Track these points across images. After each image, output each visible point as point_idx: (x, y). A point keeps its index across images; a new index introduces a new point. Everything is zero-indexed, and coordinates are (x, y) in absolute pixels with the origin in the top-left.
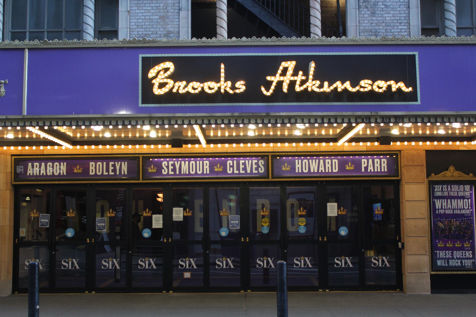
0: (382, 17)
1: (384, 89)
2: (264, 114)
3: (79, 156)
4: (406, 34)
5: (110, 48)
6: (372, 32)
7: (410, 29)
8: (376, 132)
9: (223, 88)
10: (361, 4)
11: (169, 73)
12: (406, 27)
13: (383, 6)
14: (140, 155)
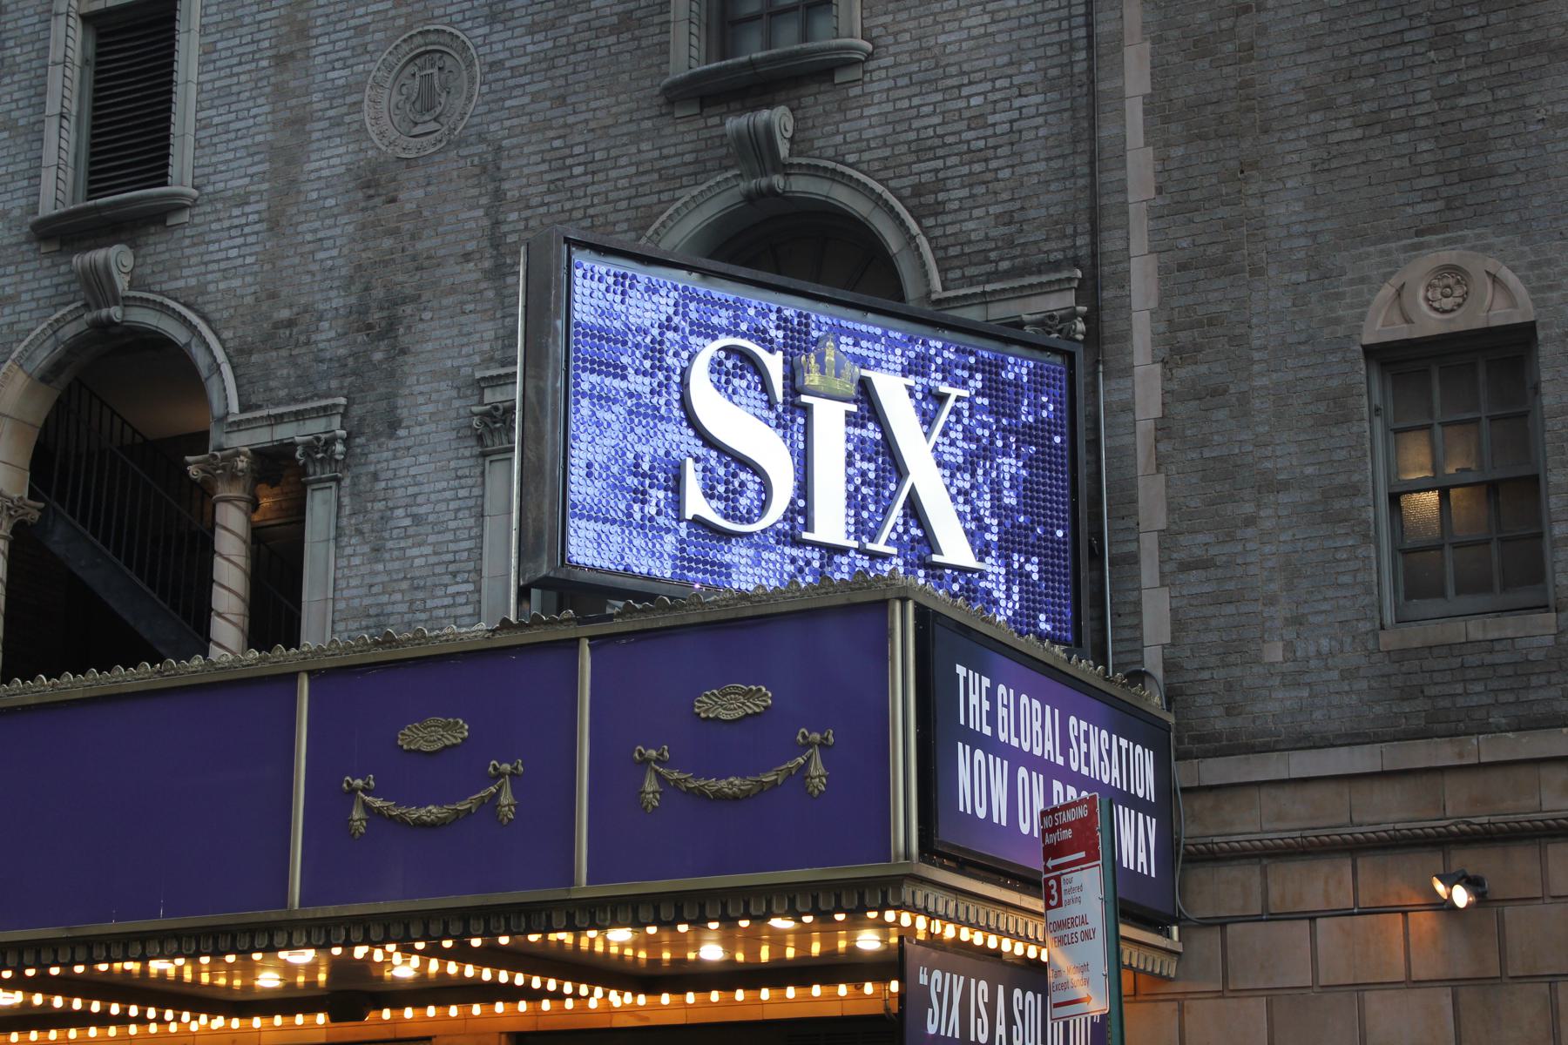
0: (404, 558)
4: (469, 609)
6: (369, 616)
7: (479, 591)
8: (322, 977)
10: (344, 522)
12: (471, 587)
13: (408, 522)
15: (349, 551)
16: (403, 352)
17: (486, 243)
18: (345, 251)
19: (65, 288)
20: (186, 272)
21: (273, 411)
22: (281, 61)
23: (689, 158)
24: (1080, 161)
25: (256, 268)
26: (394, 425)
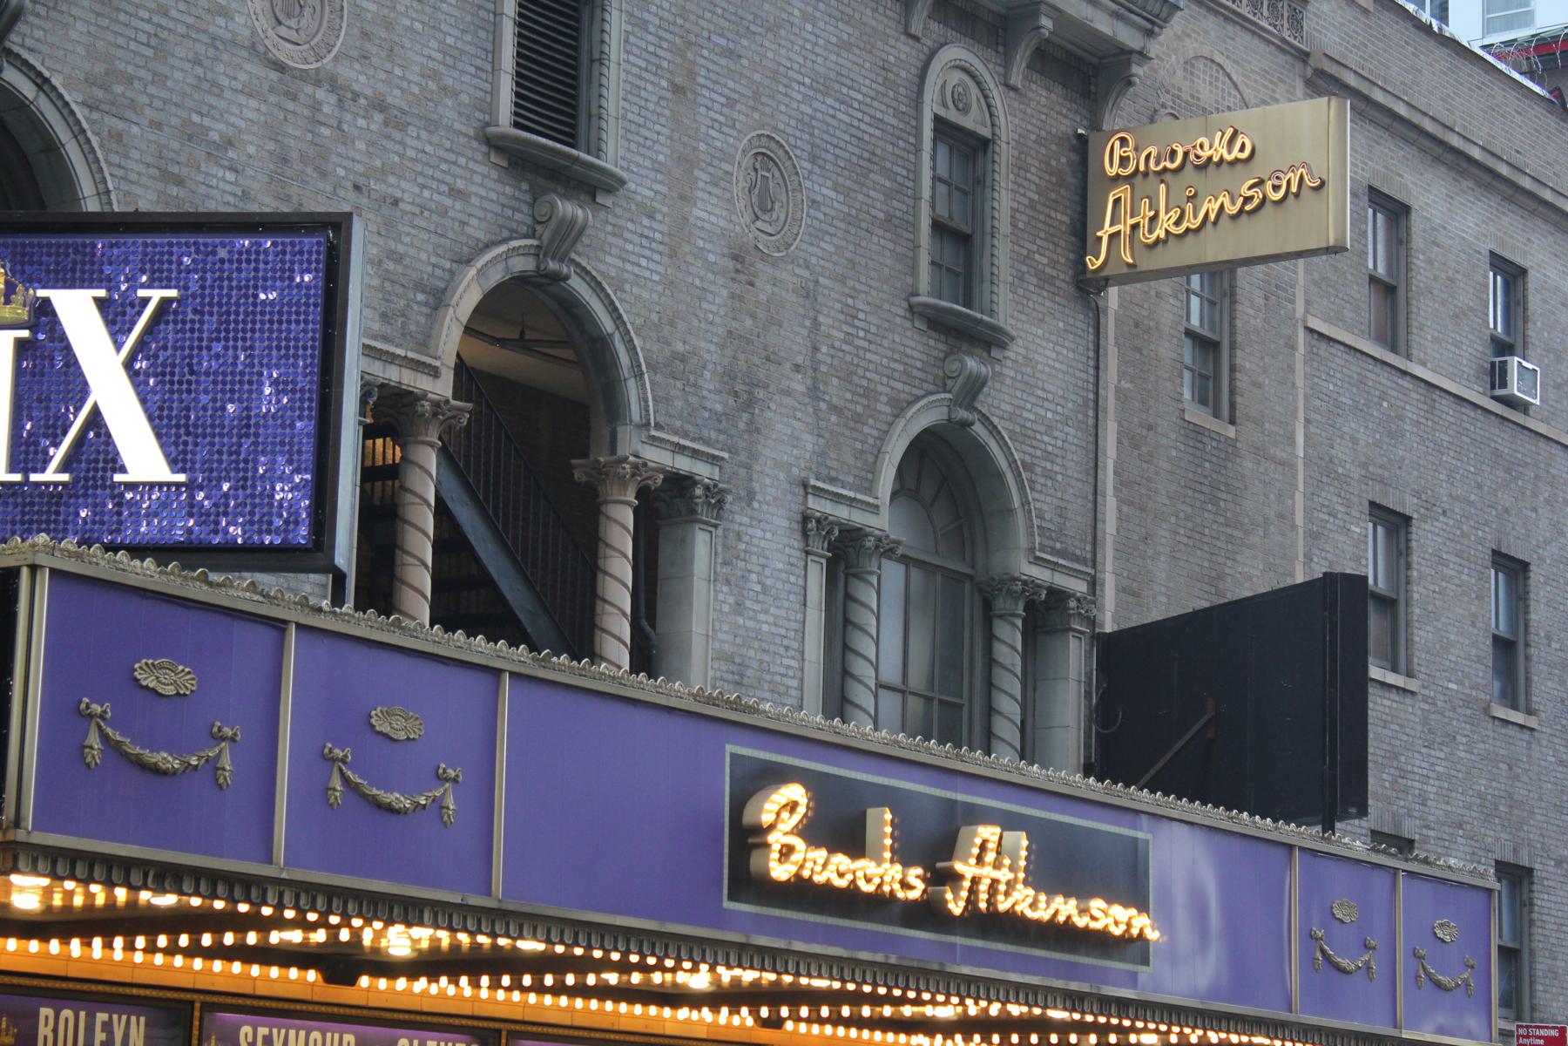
1: (1123, 927)
2: (936, 967)
3: (35, 982)
5: (670, 710)
9: (887, 879)
11: (797, 817)
14: (195, 997)
15: (721, 597)
16: (758, 431)
17: (808, 363)
18: (722, 312)
19: (510, 213)
20: (608, 259)
21: (682, 442)
22: (677, 89)
23: (919, 365)
24: (1090, 489)
25: (660, 288)
26: (751, 496)
